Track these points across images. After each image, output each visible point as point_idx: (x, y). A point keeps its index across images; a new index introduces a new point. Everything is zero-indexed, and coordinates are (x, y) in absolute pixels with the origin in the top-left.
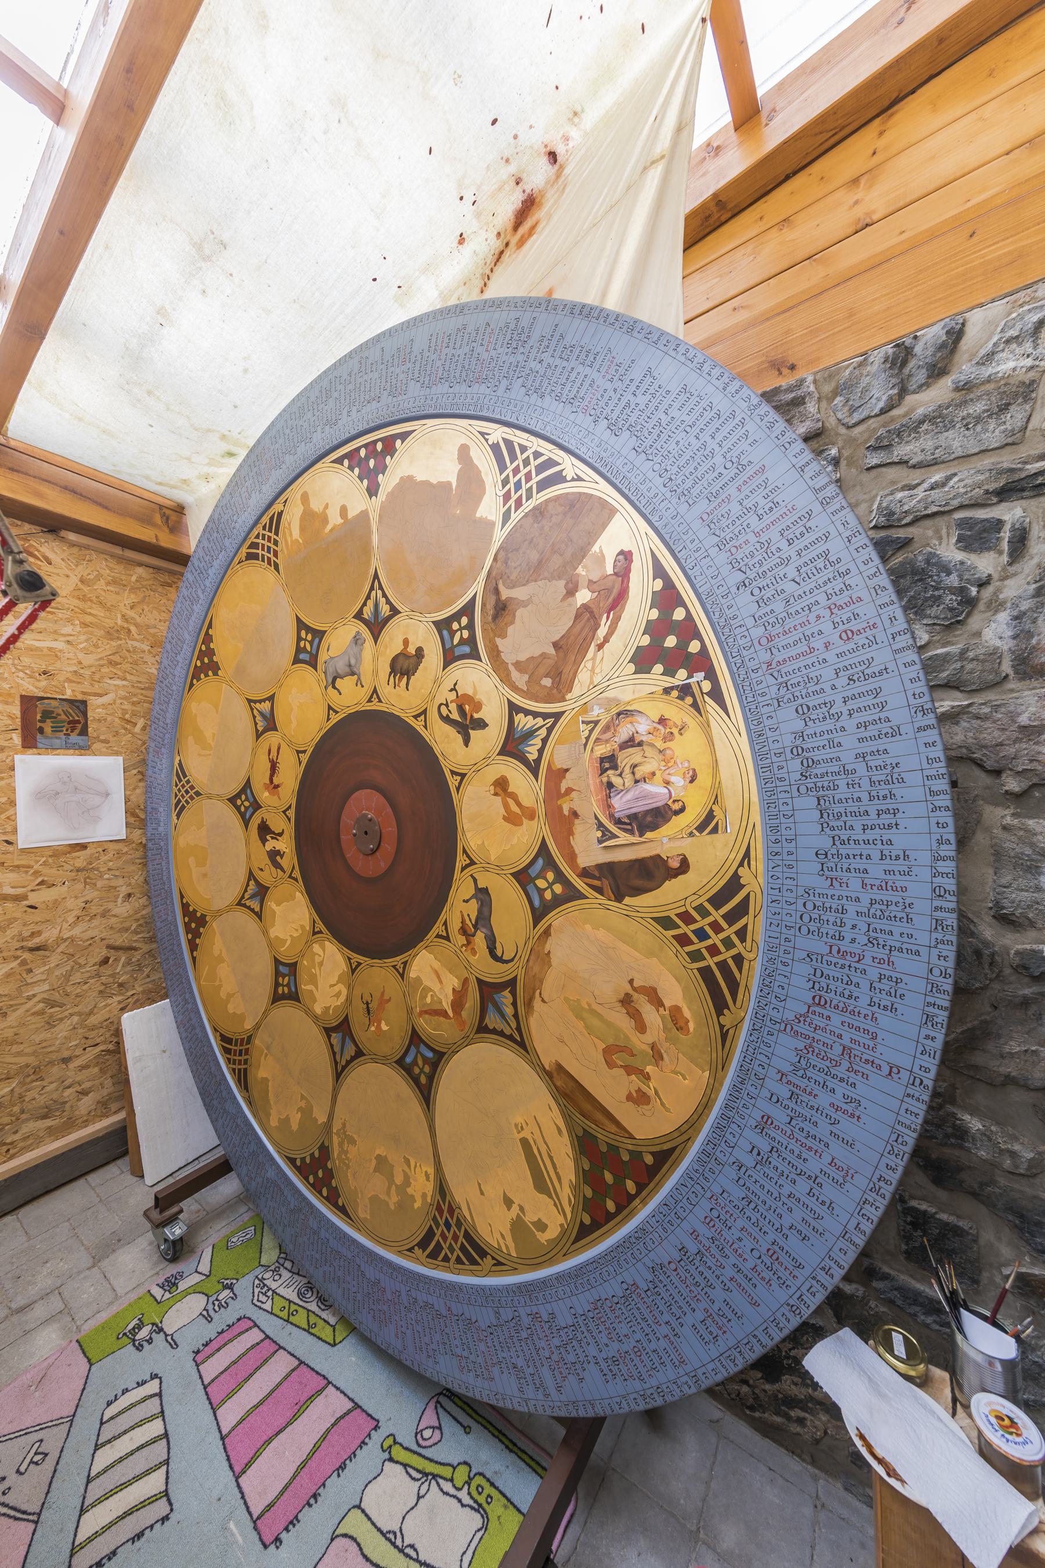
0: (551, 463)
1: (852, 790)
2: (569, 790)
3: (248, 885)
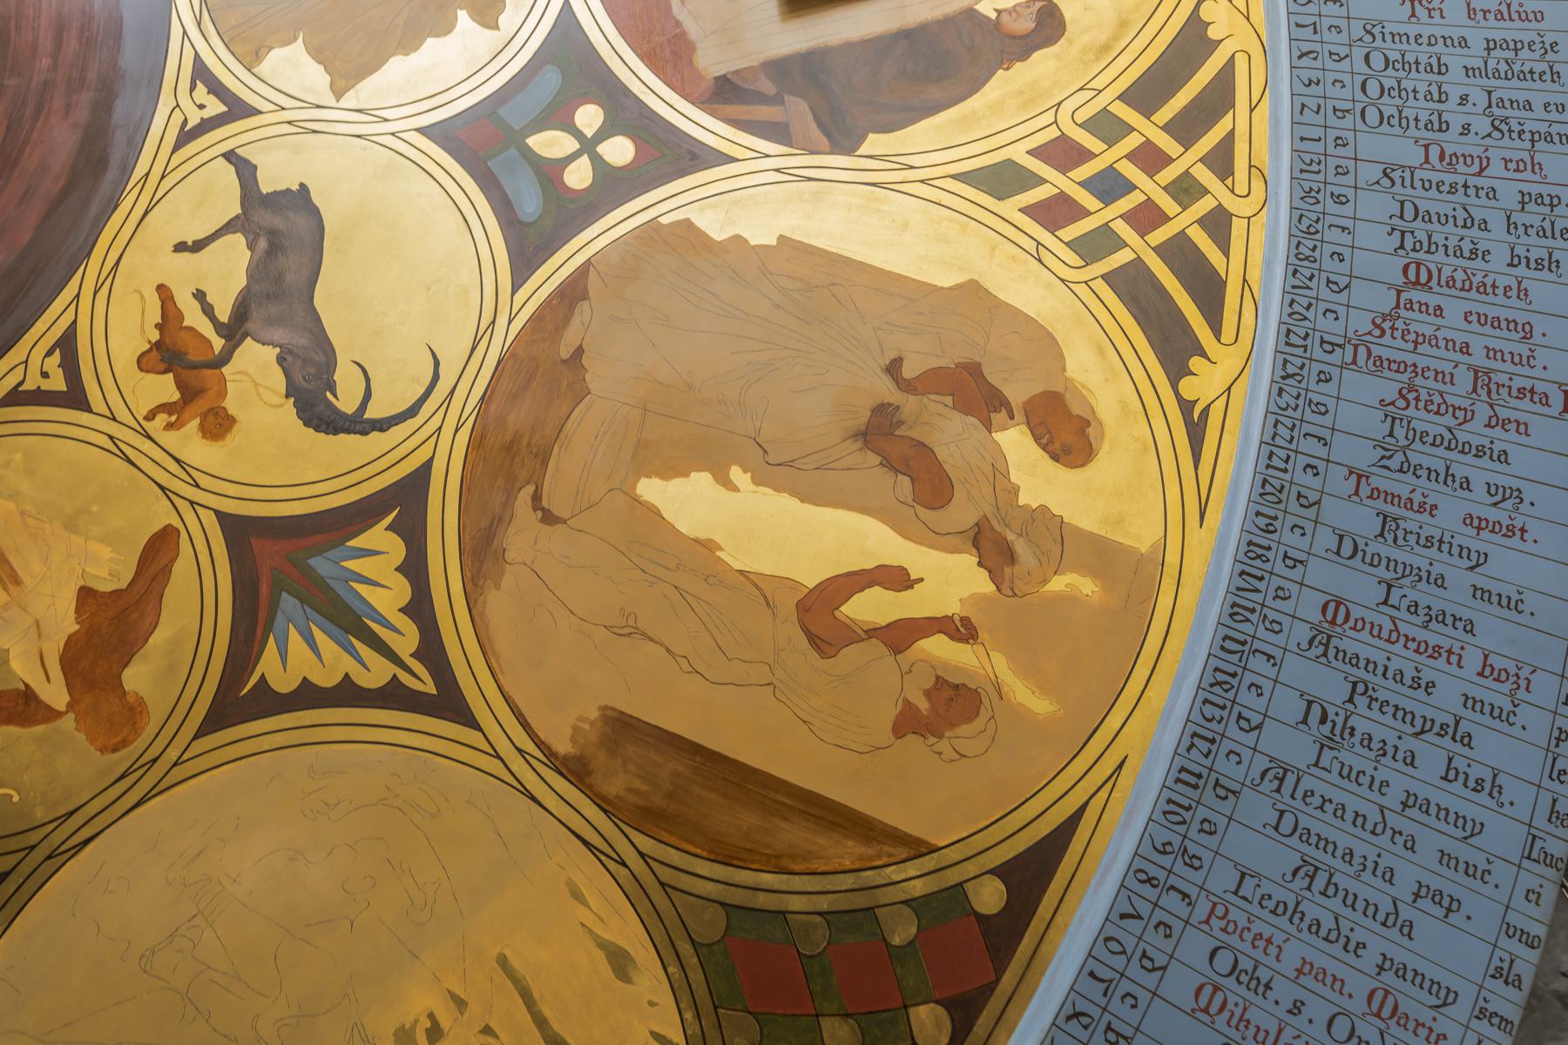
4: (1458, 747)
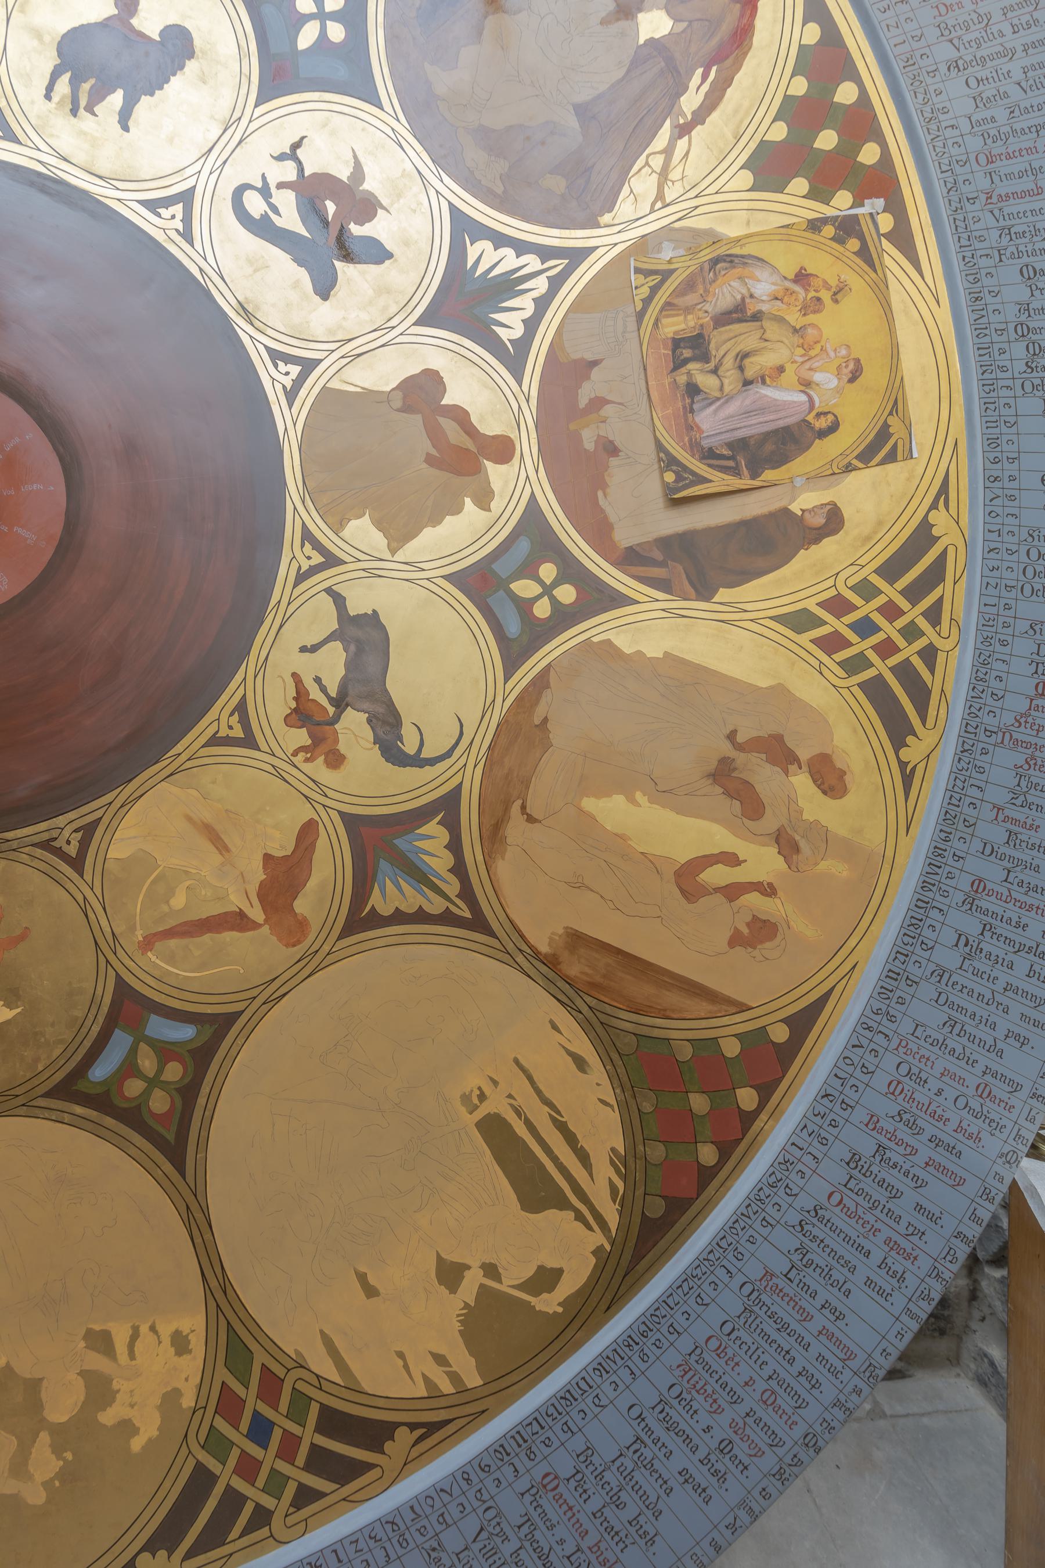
2: (598, 403)
4: (1037, 959)
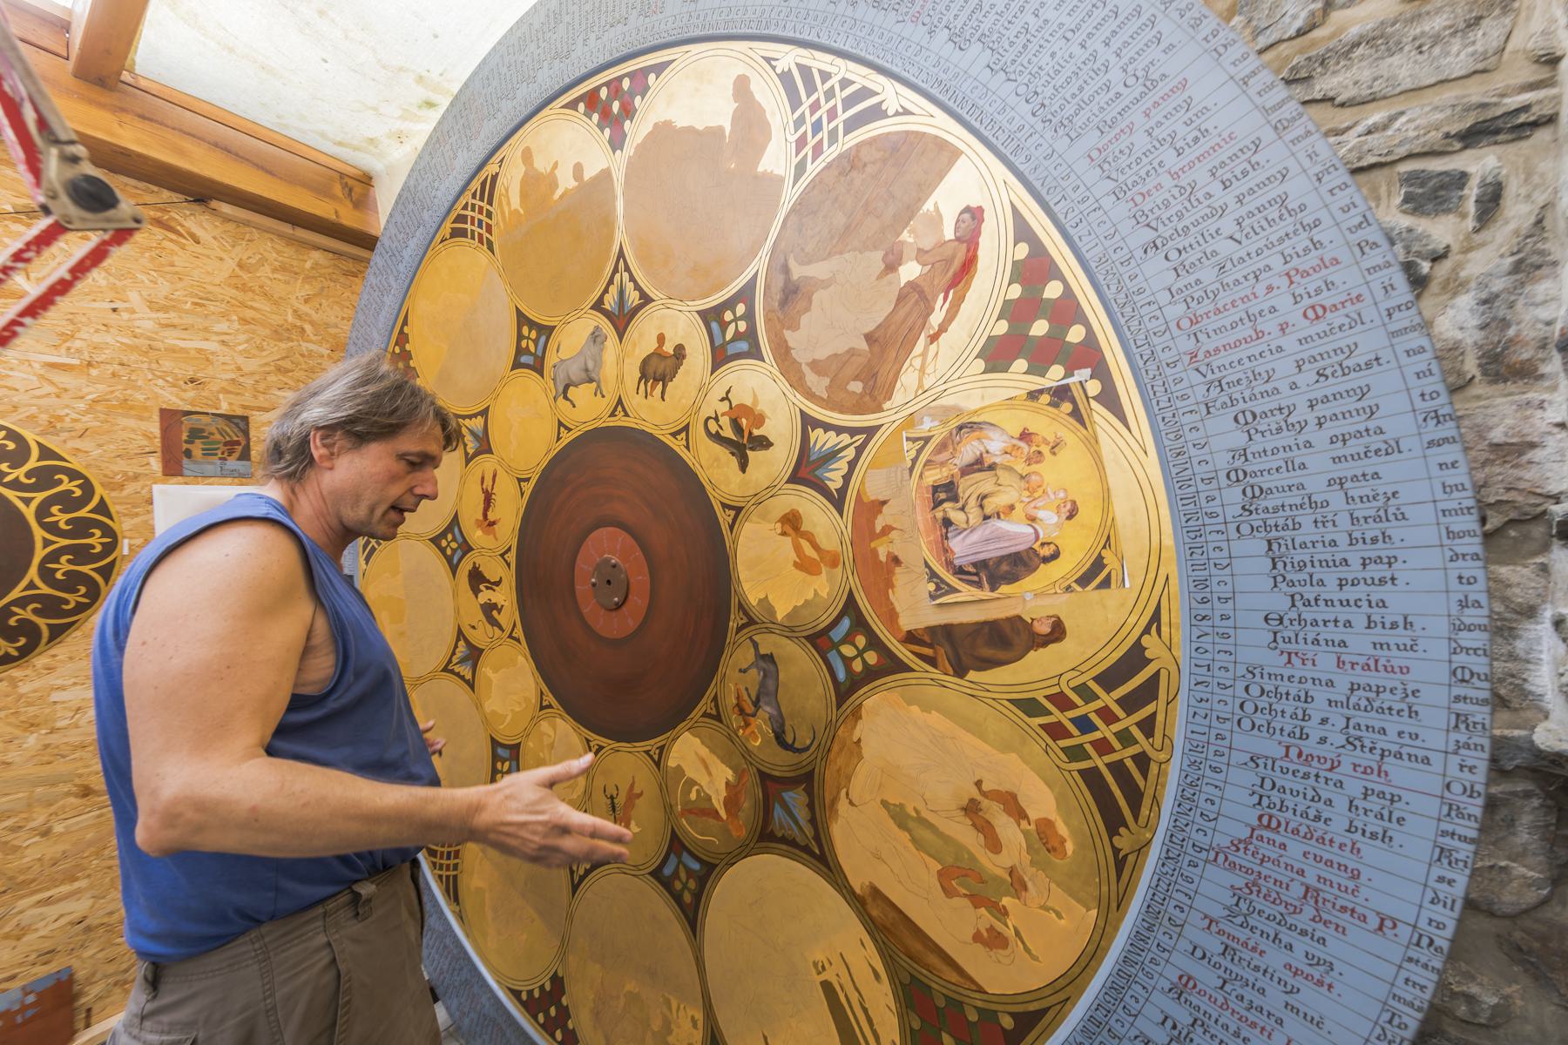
0: (865, 93)
1: (1322, 530)
2: (887, 530)
3: (456, 646)
